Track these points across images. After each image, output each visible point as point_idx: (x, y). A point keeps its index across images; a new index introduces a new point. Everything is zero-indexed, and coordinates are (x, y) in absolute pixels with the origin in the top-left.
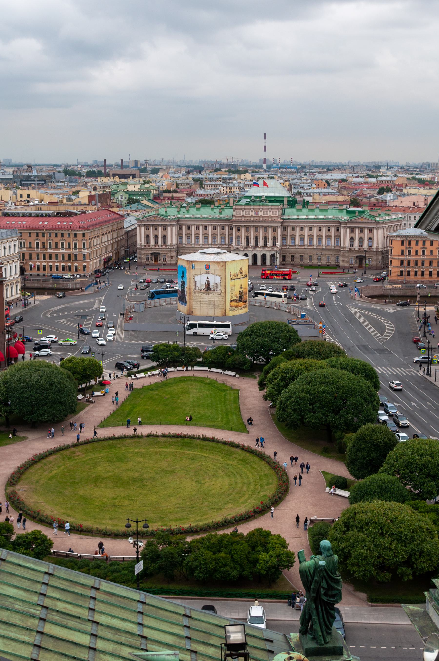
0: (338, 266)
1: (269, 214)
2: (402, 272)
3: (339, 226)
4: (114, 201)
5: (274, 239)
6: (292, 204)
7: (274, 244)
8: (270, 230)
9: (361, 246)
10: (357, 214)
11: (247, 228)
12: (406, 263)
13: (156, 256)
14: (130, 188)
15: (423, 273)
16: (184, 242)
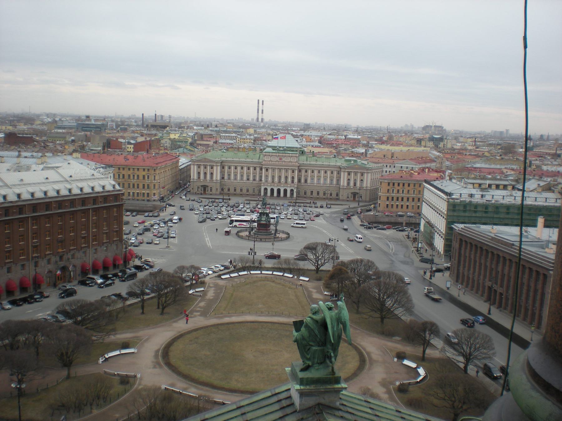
0: (338, 199)
1: (289, 159)
2: (387, 205)
4: (162, 145)
5: (293, 178)
7: (293, 182)
8: (290, 171)
9: (355, 184)
10: (352, 162)
11: (273, 169)
12: (390, 199)
13: (205, 187)
14: (172, 136)
15: (402, 205)
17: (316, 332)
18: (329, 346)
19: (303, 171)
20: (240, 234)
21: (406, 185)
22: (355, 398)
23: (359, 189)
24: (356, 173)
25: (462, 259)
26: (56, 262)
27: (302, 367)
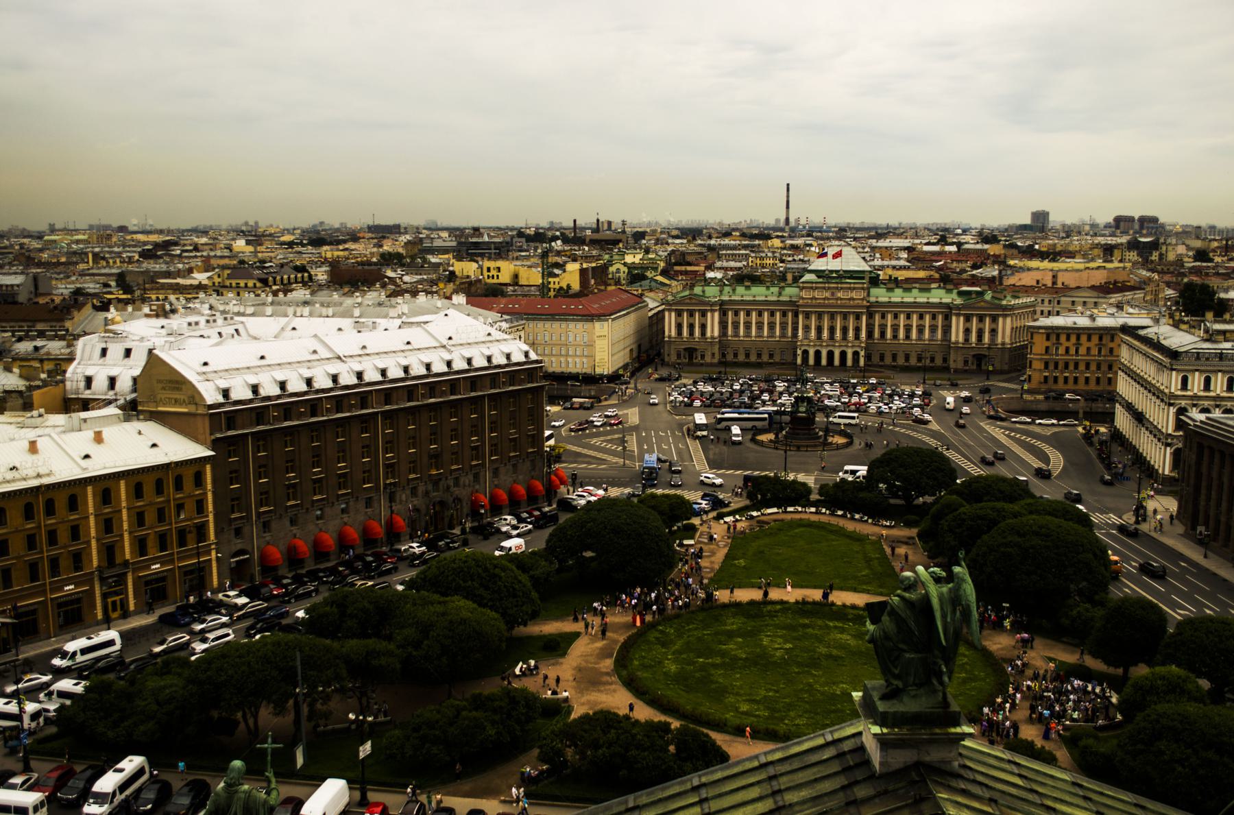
0: (946, 369)
3: (948, 311)
5: (857, 330)
6: (875, 281)
7: (857, 337)
13: (691, 352)
14: (629, 259)
15: (1076, 379)
16: (730, 333)
17: (912, 624)
18: (936, 652)
19: (877, 317)
20: (760, 438)
21: (1084, 338)
22: (989, 755)
23: (989, 348)
24: (981, 319)
25: (1204, 484)
26: (427, 493)
27: (884, 691)
